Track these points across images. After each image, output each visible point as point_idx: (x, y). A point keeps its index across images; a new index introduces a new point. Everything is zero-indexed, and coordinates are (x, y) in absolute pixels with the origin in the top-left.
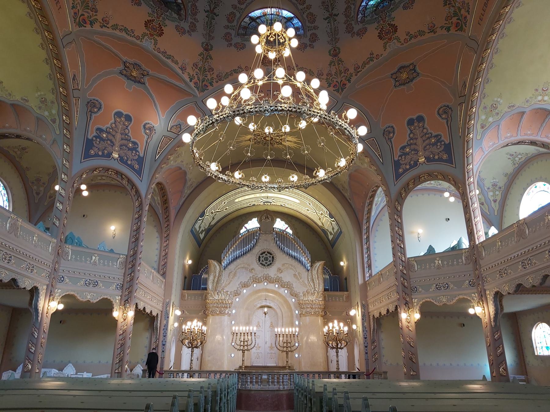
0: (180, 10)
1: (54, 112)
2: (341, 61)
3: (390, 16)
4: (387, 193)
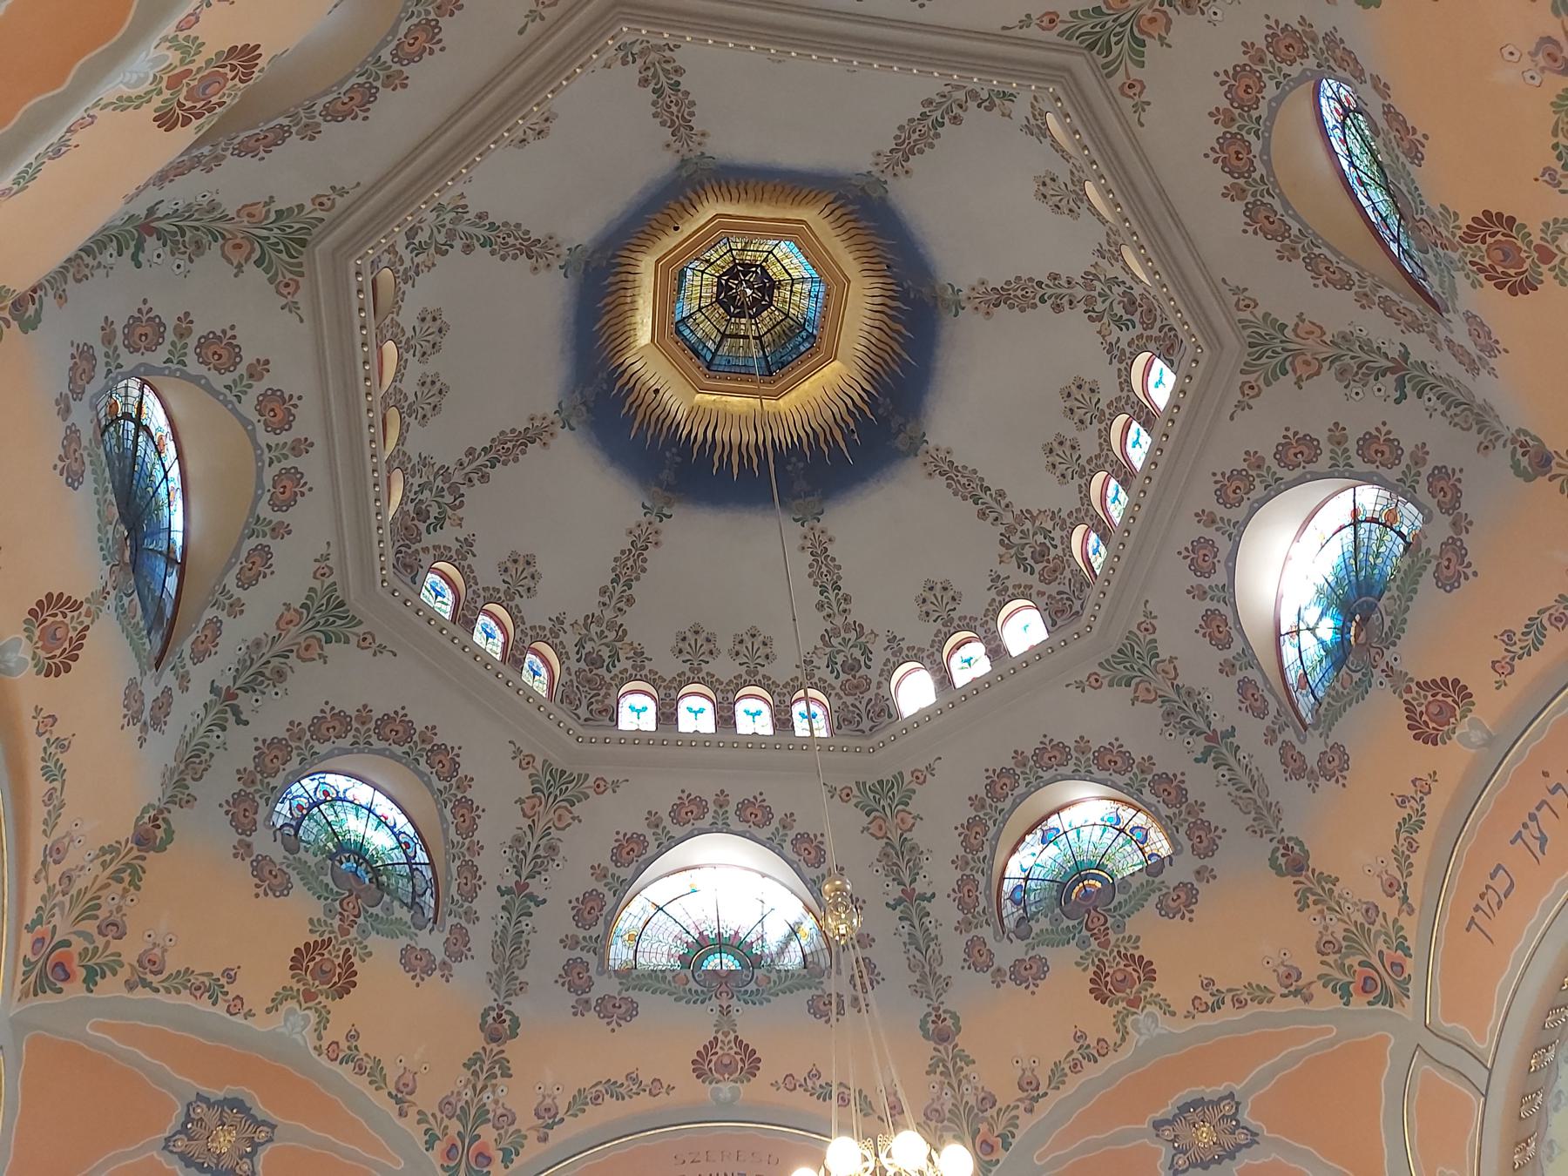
3: (364, 933)
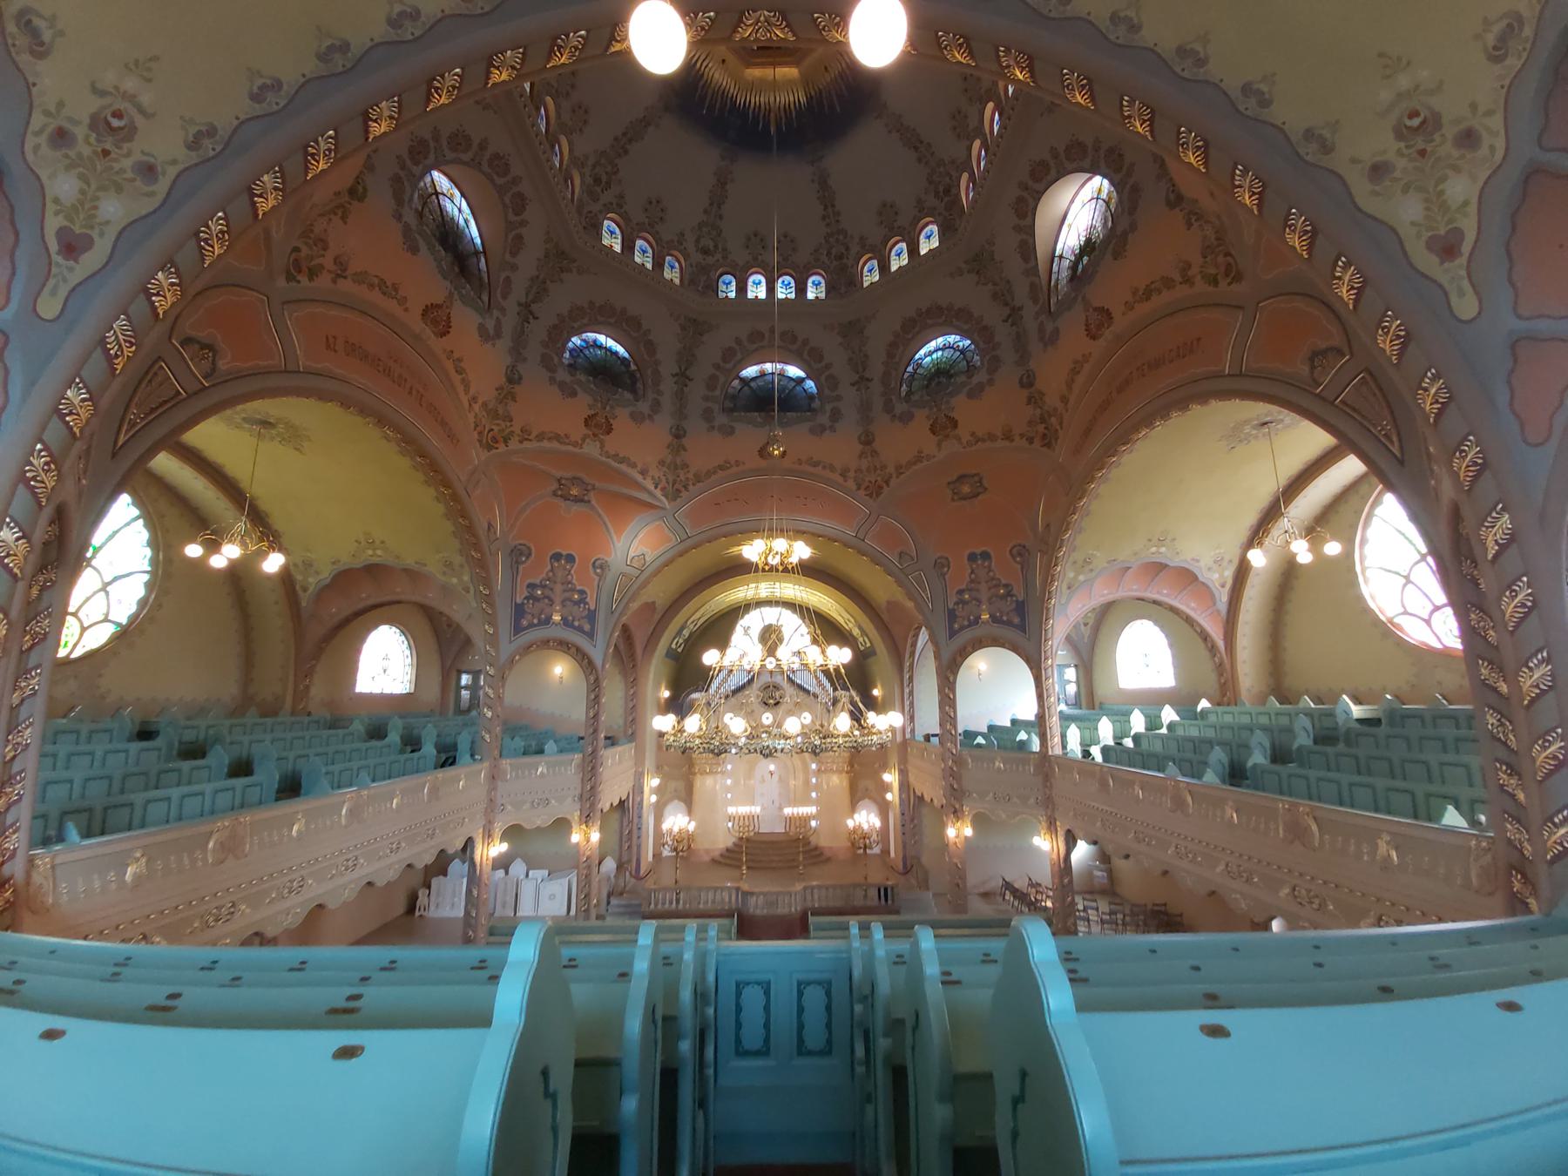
0: (634, 383)
1: (466, 578)
2: (875, 453)
4: (937, 656)
